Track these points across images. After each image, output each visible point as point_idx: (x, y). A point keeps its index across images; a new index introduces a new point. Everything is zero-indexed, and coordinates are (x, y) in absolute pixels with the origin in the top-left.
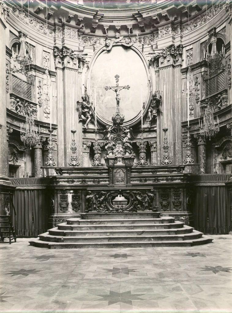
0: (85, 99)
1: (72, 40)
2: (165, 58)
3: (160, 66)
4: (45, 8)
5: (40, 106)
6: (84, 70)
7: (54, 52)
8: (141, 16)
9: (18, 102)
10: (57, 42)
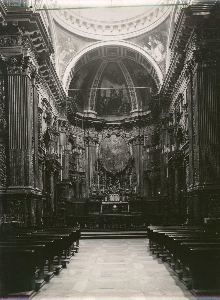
0: (99, 160)
1: (92, 133)
2: (136, 141)
3: (134, 144)
4: (81, 121)
5: (78, 165)
6: (98, 145)
7: (84, 139)
8: (124, 121)
9: (70, 165)
10: (85, 134)
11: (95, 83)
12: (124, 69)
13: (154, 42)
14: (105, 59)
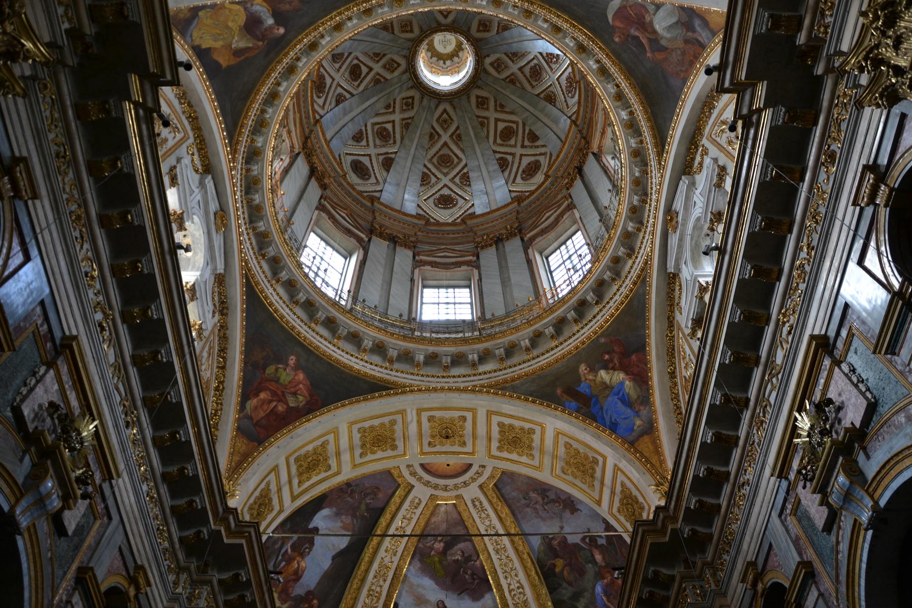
11: (375, 577)
12: (487, 523)
13: (599, 379)
14: (420, 479)
